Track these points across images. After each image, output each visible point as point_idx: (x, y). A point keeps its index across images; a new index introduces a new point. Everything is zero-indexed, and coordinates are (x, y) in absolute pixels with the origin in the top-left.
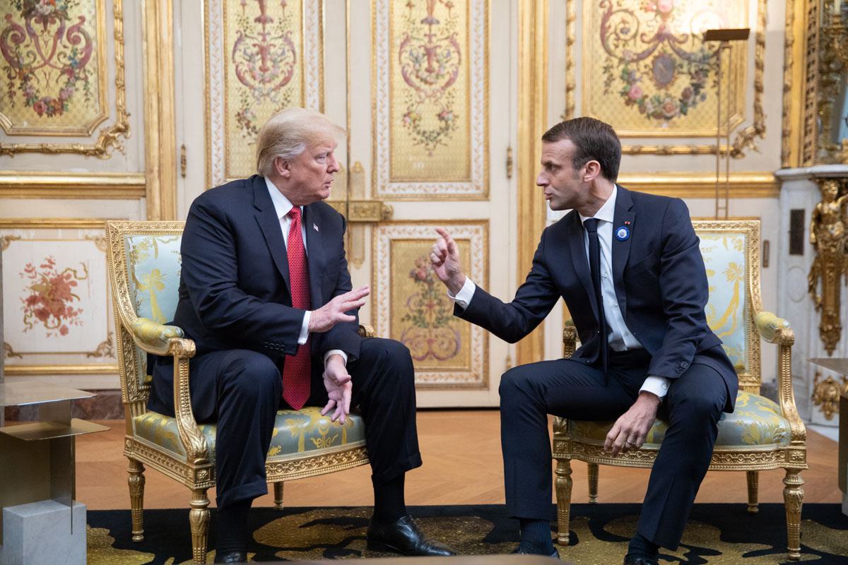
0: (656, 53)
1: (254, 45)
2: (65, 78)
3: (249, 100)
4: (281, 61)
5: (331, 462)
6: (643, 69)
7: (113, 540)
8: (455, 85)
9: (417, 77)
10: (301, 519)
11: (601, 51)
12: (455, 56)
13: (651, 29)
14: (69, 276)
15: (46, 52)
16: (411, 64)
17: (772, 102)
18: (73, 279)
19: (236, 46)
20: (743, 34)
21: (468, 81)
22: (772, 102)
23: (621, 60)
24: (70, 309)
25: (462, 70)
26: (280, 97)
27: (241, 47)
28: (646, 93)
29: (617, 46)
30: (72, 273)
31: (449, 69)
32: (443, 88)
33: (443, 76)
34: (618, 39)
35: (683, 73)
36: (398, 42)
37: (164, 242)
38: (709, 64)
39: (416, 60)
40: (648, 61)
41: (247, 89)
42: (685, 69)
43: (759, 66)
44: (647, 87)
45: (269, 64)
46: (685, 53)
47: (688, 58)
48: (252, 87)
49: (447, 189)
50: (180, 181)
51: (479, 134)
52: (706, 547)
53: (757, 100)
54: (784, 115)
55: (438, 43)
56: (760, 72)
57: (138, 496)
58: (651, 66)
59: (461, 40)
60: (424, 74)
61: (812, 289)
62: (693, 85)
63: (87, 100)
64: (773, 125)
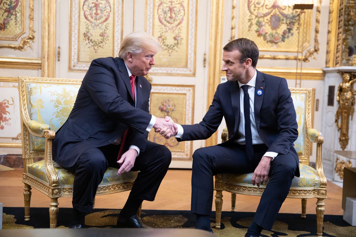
1: (93, 3)
2: (6, 14)
3: (89, 27)
4: (104, 10)
5: (115, 188)
6: (266, 21)
7: (16, 220)
8: (182, 25)
9: (165, 20)
10: (102, 214)
11: (248, 12)
12: (182, 11)
13: (270, 3)
14: (5, 103)
16: (163, 14)
17: (322, 38)
18: (7, 104)
19: (84, 3)
20: (310, 7)
21: (188, 23)
22: (322, 38)
23: (256, 16)
24: (5, 118)
25: (185, 18)
26: (103, 27)
28: (267, 31)
29: (255, 10)
30: (7, 102)
31: (179, 17)
32: (177, 26)
33: (177, 20)
34: (255, 7)
35: (283, 23)
36: (157, 4)
37: (44, 87)
38: (295, 20)
39: (165, 13)
40: (268, 17)
41: (88, 22)
42: (285, 22)
43: (318, 21)
44: (267, 29)
45: (99, 12)
46: (285, 14)
47: (286, 16)
48: (91, 22)
49: (177, 71)
50: (57, 62)
51: (192, 47)
52: (281, 232)
53: (316, 36)
54: (328, 44)
55: (175, 6)
56: (318, 24)
57: (28, 201)
58: (270, 20)
59: (185, 5)
60: (169, 19)
61: (336, 121)
62: (288, 29)
63: (16, 24)
64: (323, 48)
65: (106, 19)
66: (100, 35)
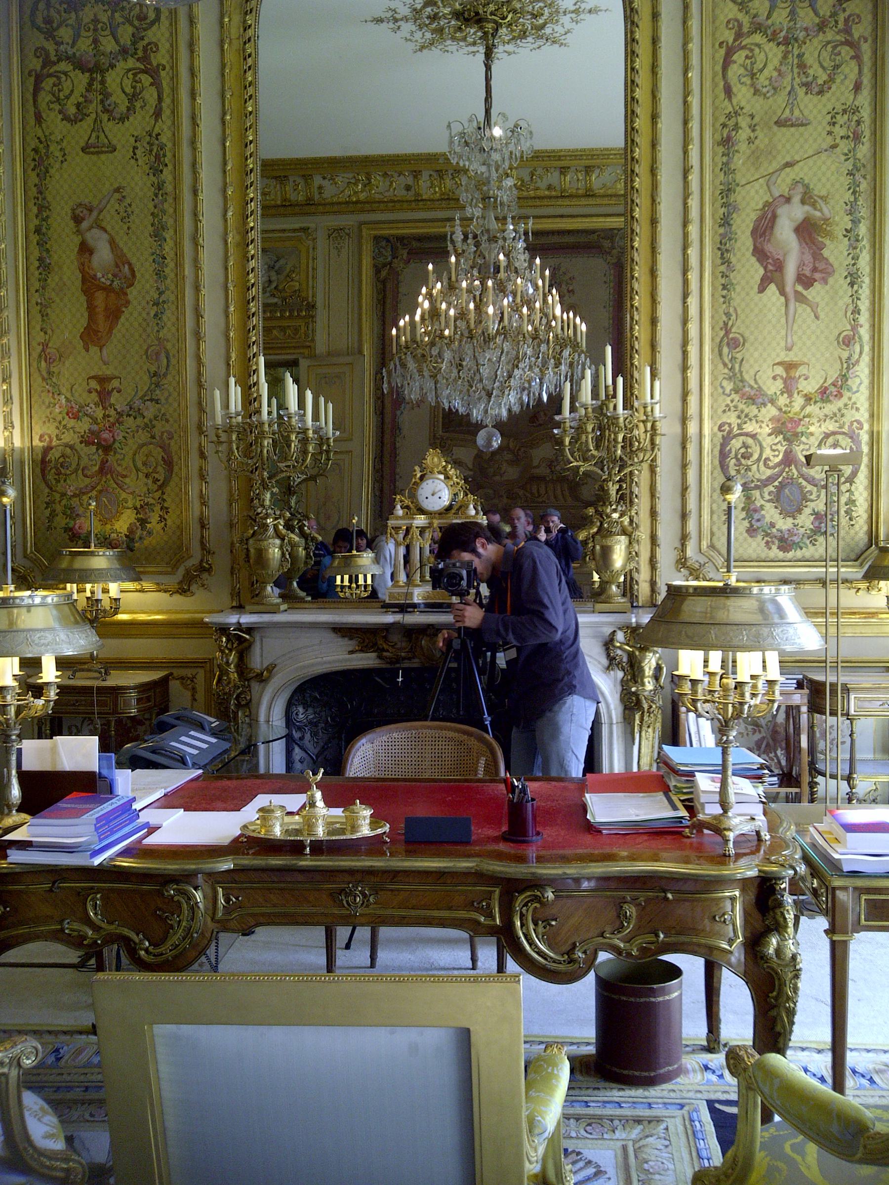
0: (99, 488)
11: (43, 486)
29: (58, 481)
34: (59, 474)
35: (128, 508)
62: (138, 520)
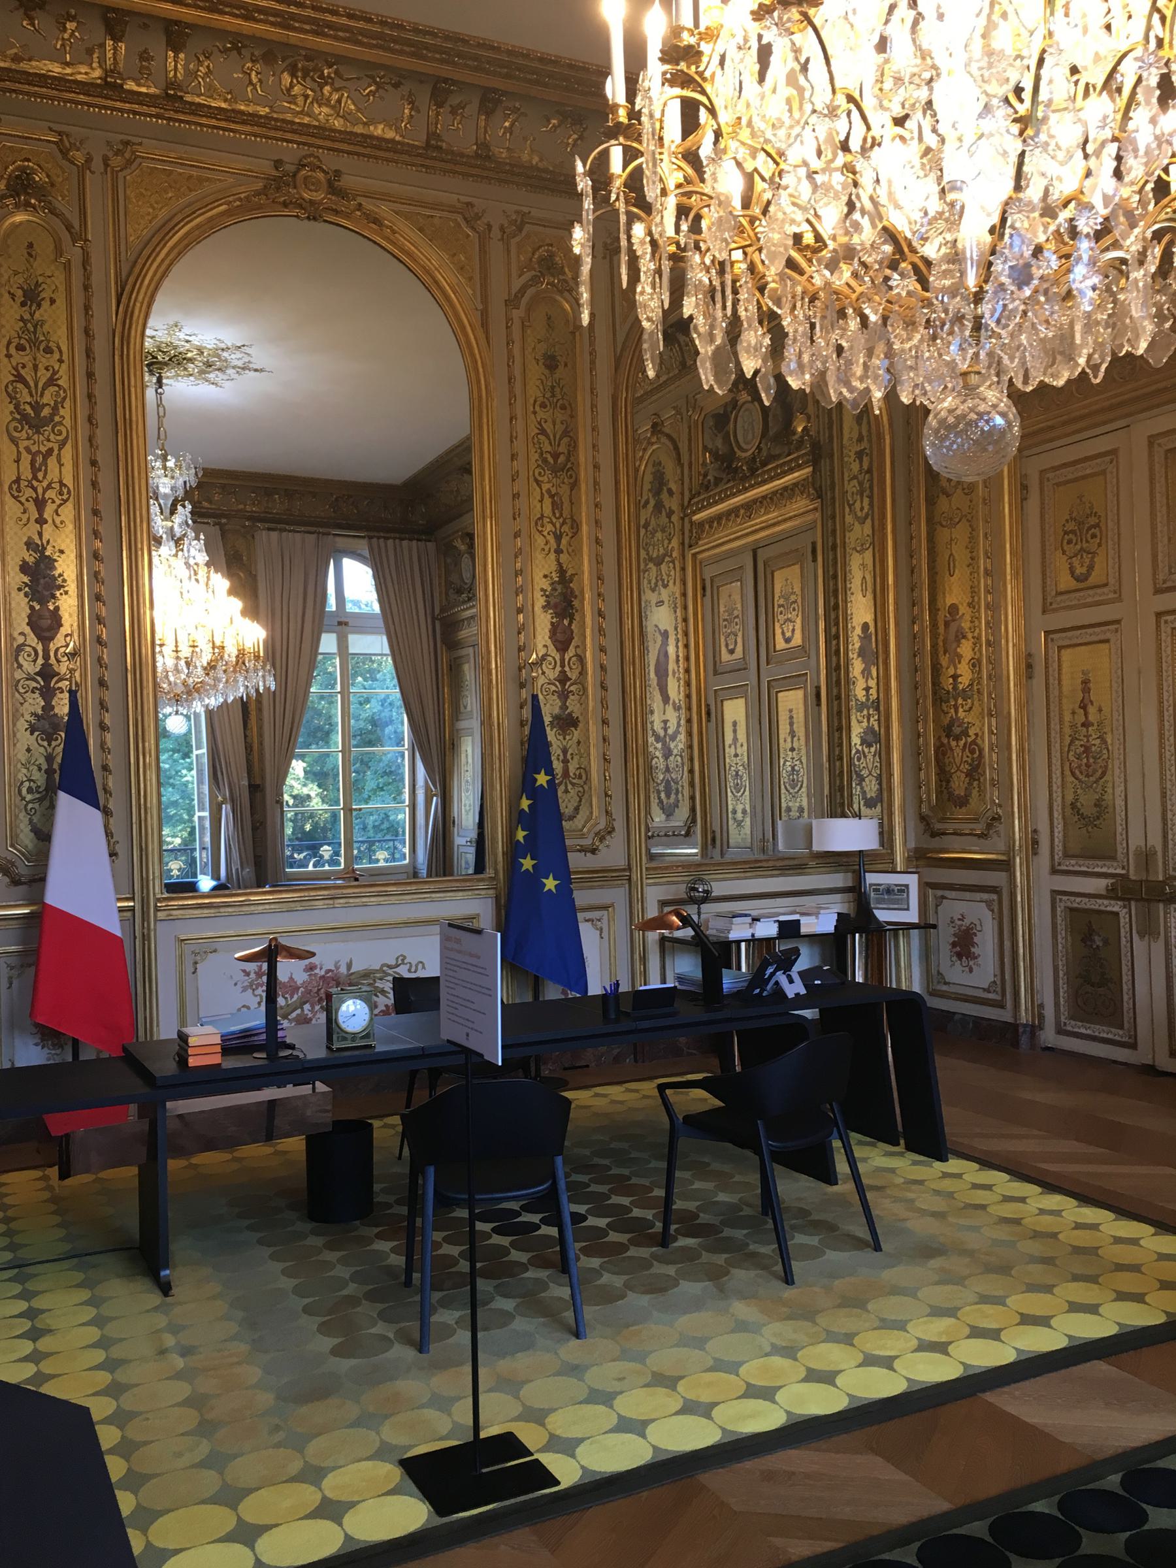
15: (958, 761)
27: (1073, 748)
41: (1076, 782)
45: (1091, 760)
48: (1080, 781)
65: (1104, 774)
66: (1096, 805)
